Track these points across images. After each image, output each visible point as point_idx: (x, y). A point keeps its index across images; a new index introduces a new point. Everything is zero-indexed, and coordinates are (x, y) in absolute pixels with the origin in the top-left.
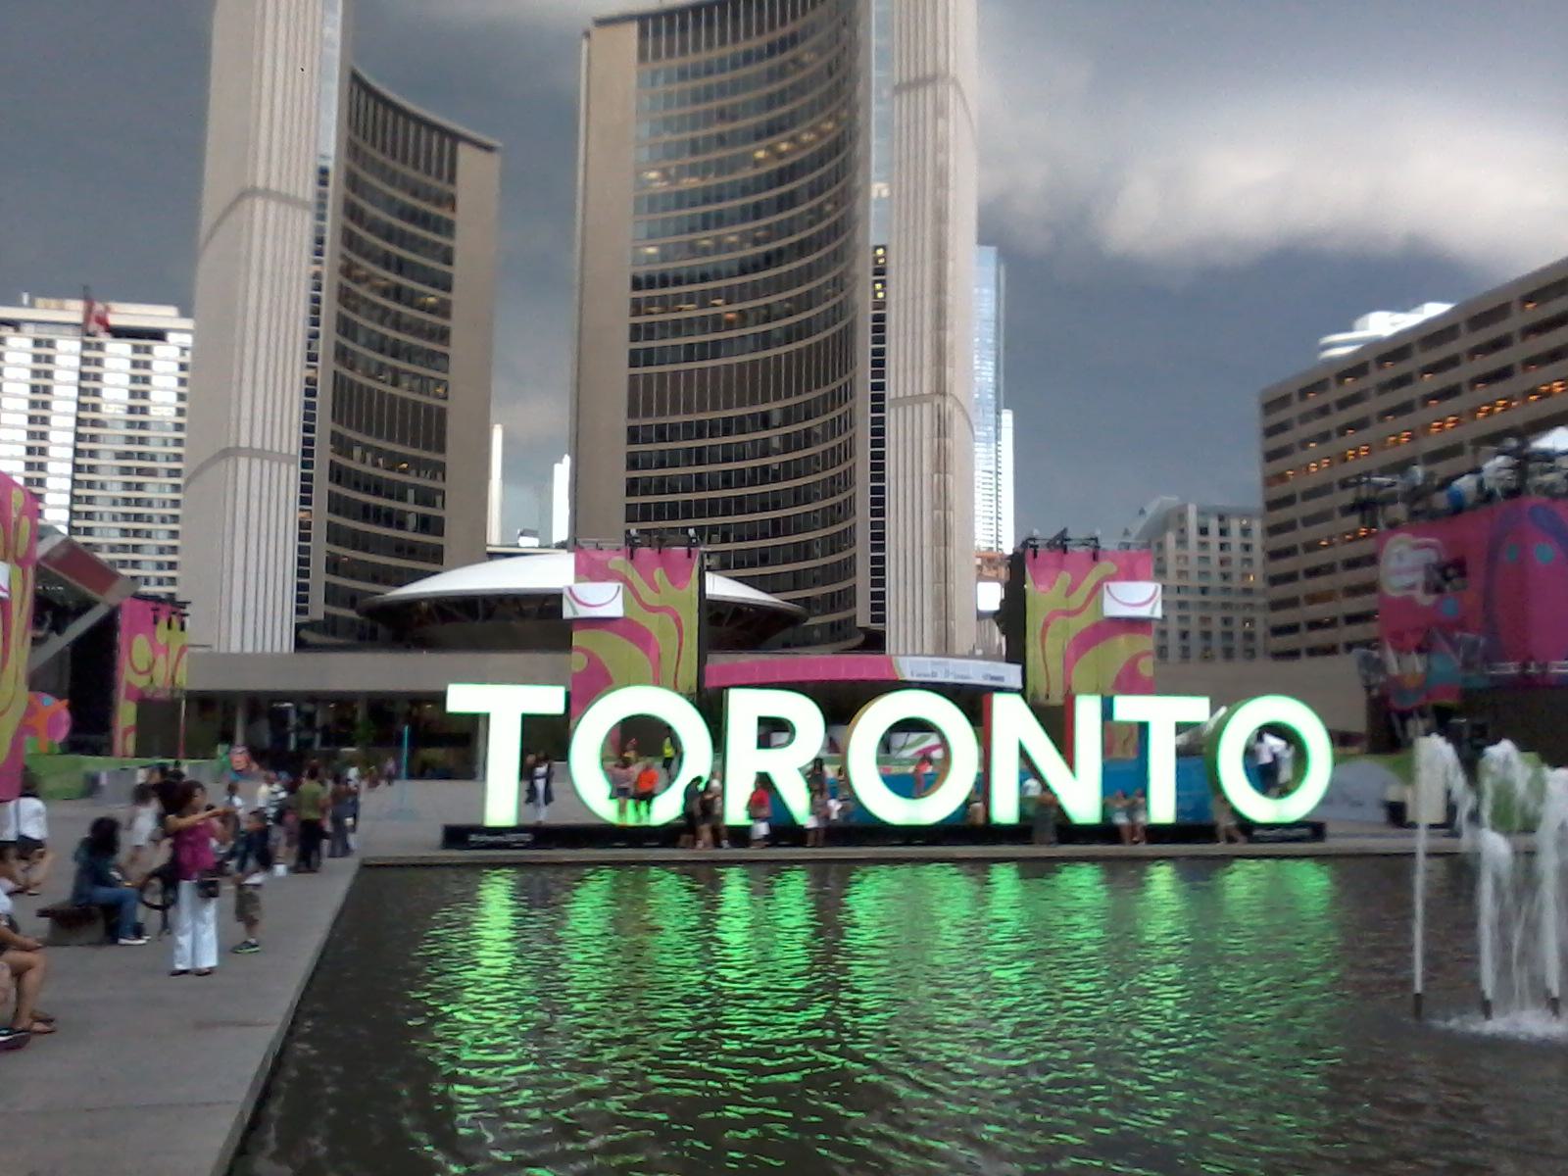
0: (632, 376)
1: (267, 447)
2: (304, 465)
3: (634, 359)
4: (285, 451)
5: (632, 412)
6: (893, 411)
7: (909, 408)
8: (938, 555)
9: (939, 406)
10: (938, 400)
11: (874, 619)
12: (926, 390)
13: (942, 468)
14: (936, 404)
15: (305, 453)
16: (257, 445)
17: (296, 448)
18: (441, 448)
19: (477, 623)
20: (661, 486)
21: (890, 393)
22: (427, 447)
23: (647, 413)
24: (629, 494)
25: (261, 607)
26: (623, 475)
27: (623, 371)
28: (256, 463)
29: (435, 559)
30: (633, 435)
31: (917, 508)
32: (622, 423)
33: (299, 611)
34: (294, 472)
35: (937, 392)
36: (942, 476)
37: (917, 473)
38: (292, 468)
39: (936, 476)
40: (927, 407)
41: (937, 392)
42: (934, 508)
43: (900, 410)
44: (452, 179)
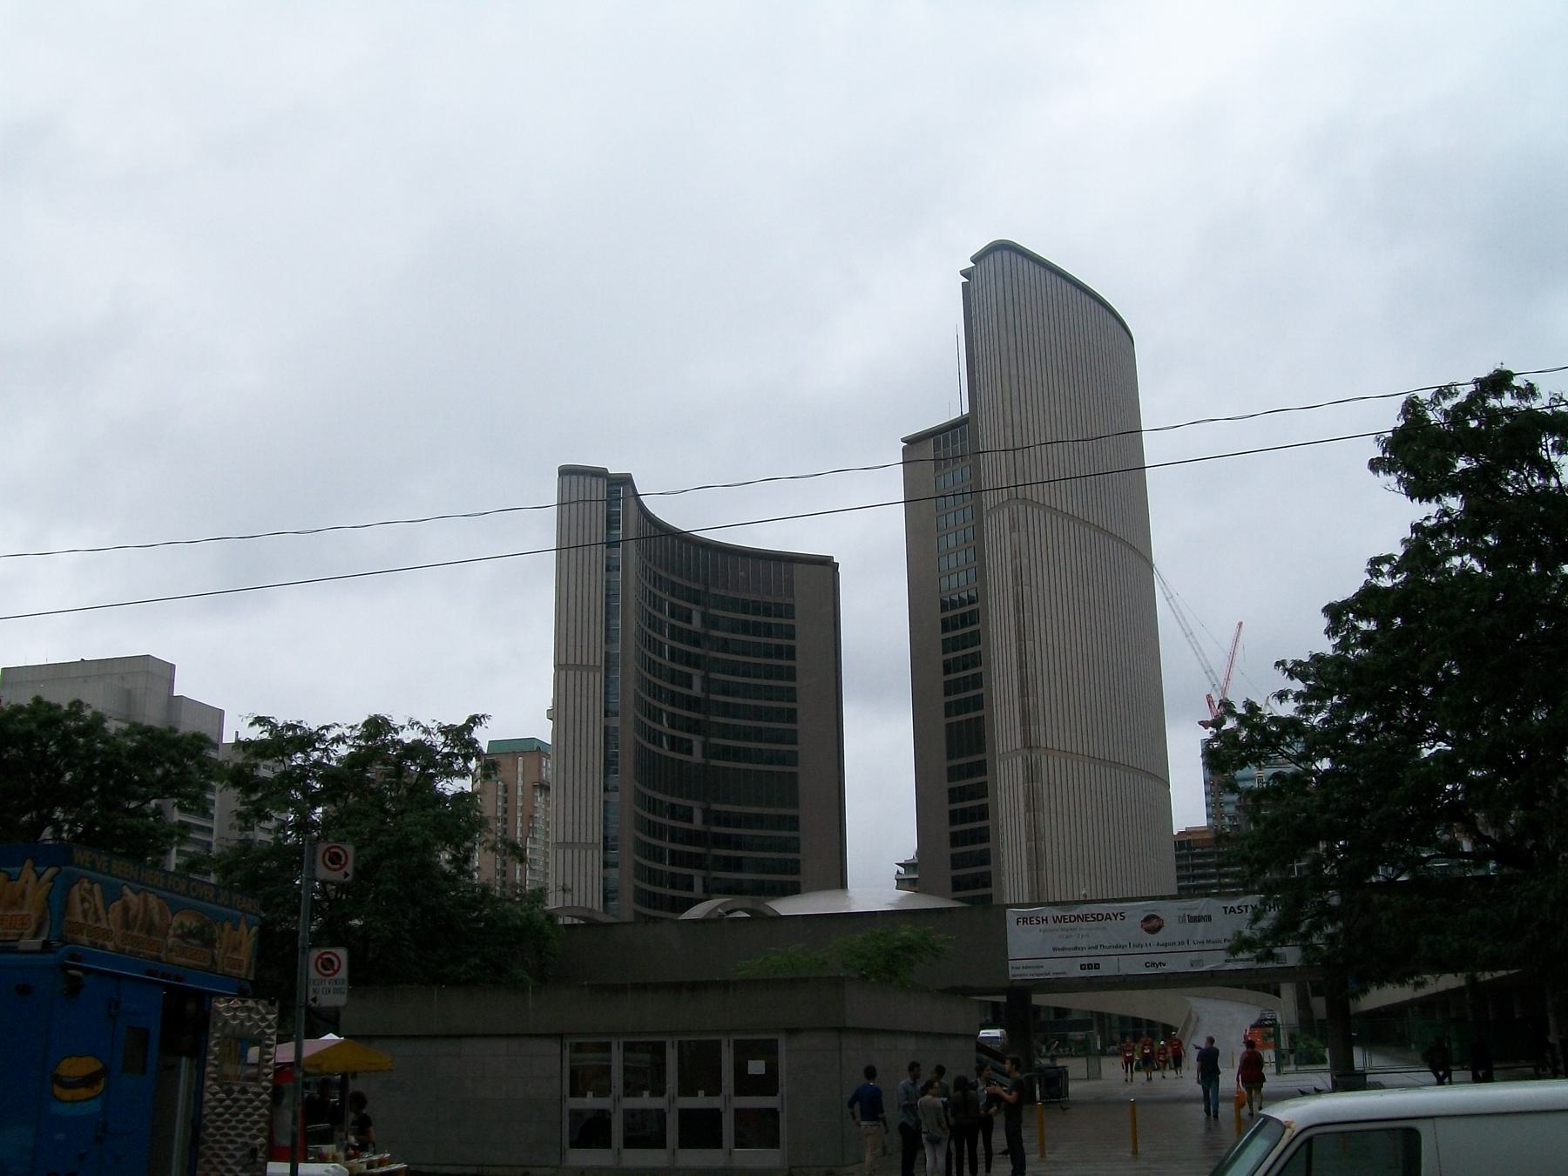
0: (948, 726)
5: (950, 756)
8: (1032, 879)
9: (1027, 758)
10: (1026, 752)
14: (1025, 757)
16: (569, 839)
18: (794, 803)
28: (569, 852)
29: (793, 890)
36: (1032, 813)
38: (596, 853)
39: (1027, 814)
40: (1020, 759)
42: (1028, 839)
44: (792, 596)
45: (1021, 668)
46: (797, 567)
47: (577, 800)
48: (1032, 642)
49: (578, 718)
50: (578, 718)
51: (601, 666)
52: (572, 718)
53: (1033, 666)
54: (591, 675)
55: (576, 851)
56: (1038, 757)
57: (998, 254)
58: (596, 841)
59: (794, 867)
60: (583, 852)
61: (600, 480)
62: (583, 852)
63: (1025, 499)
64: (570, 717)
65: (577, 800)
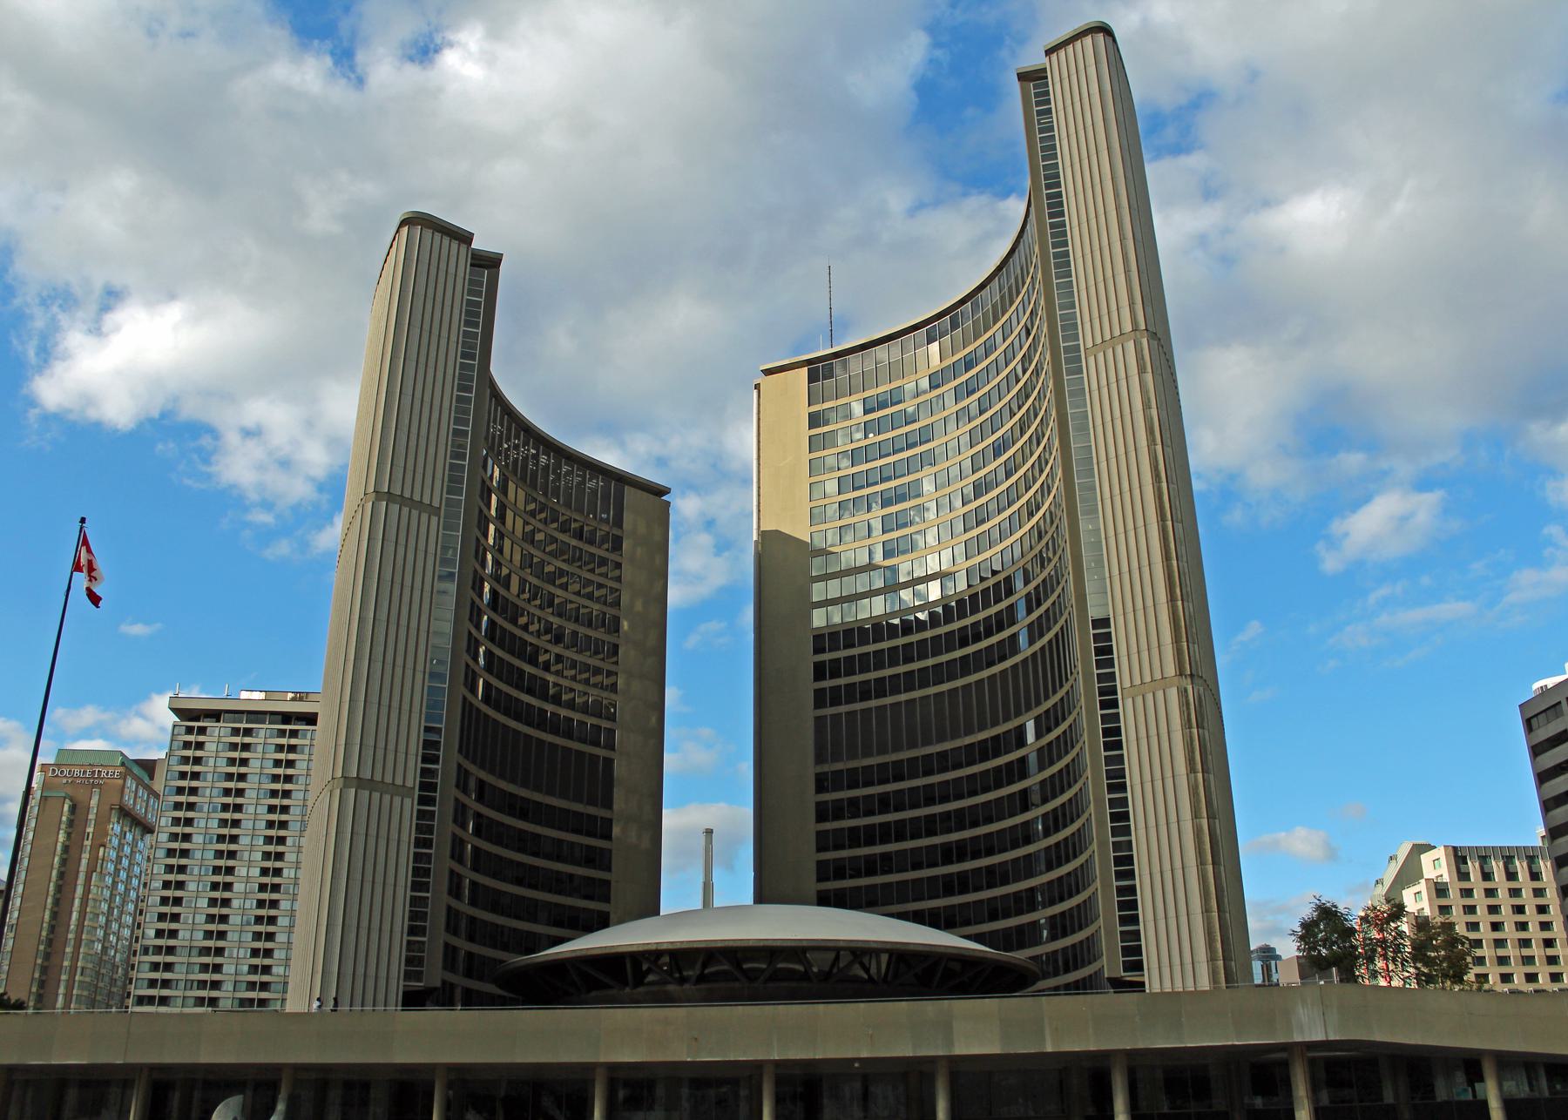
0: (819, 721)
1: (378, 777)
2: (423, 800)
3: (820, 699)
4: (399, 782)
5: (820, 758)
6: (1129, 702)
7: (1150, 697)
9: (1186, 690)
11: (1129, 967)
12: (1171, 670)
13: (1199, 767)
15: (424, 786)
17: (413, 780)
19: (627, 990)
20: (854, 808)
21: (1123, 681)
22: (592, 802)
23: (836, 758)
24: (819, 849)
25: (360, 970)
26: (812, 827)
27: (810, 713)
30: (821, 784)
31: (1173, 818)
32: (811, 770)
33: (408, 976)
34: (410, 806)
35: (1181, 675)
36: (1200, 775)
37: (1168, 774)
38: (408, 802)
40: (1173, 694)
41: (1181, 675)
43: (1139, 700)
45: (1167, 560)
46: (630, 493)
47: (384, 710)
48: (1180, 525)
49: (398, 579)
50: (398, 579)
51: (440, 508)
52: (389, 578)
53: (1185, 559)
54: (425, 517)
55: (376, 795)
56: (1201, 689)
57: (1100, 37)
58: (409, 783)
59: (602, 890)
60: (387, 798)
61: (463, 248)
62: (387, 798)
63: (1155, 334)
64: (388, 576)
65: (384, 710)
